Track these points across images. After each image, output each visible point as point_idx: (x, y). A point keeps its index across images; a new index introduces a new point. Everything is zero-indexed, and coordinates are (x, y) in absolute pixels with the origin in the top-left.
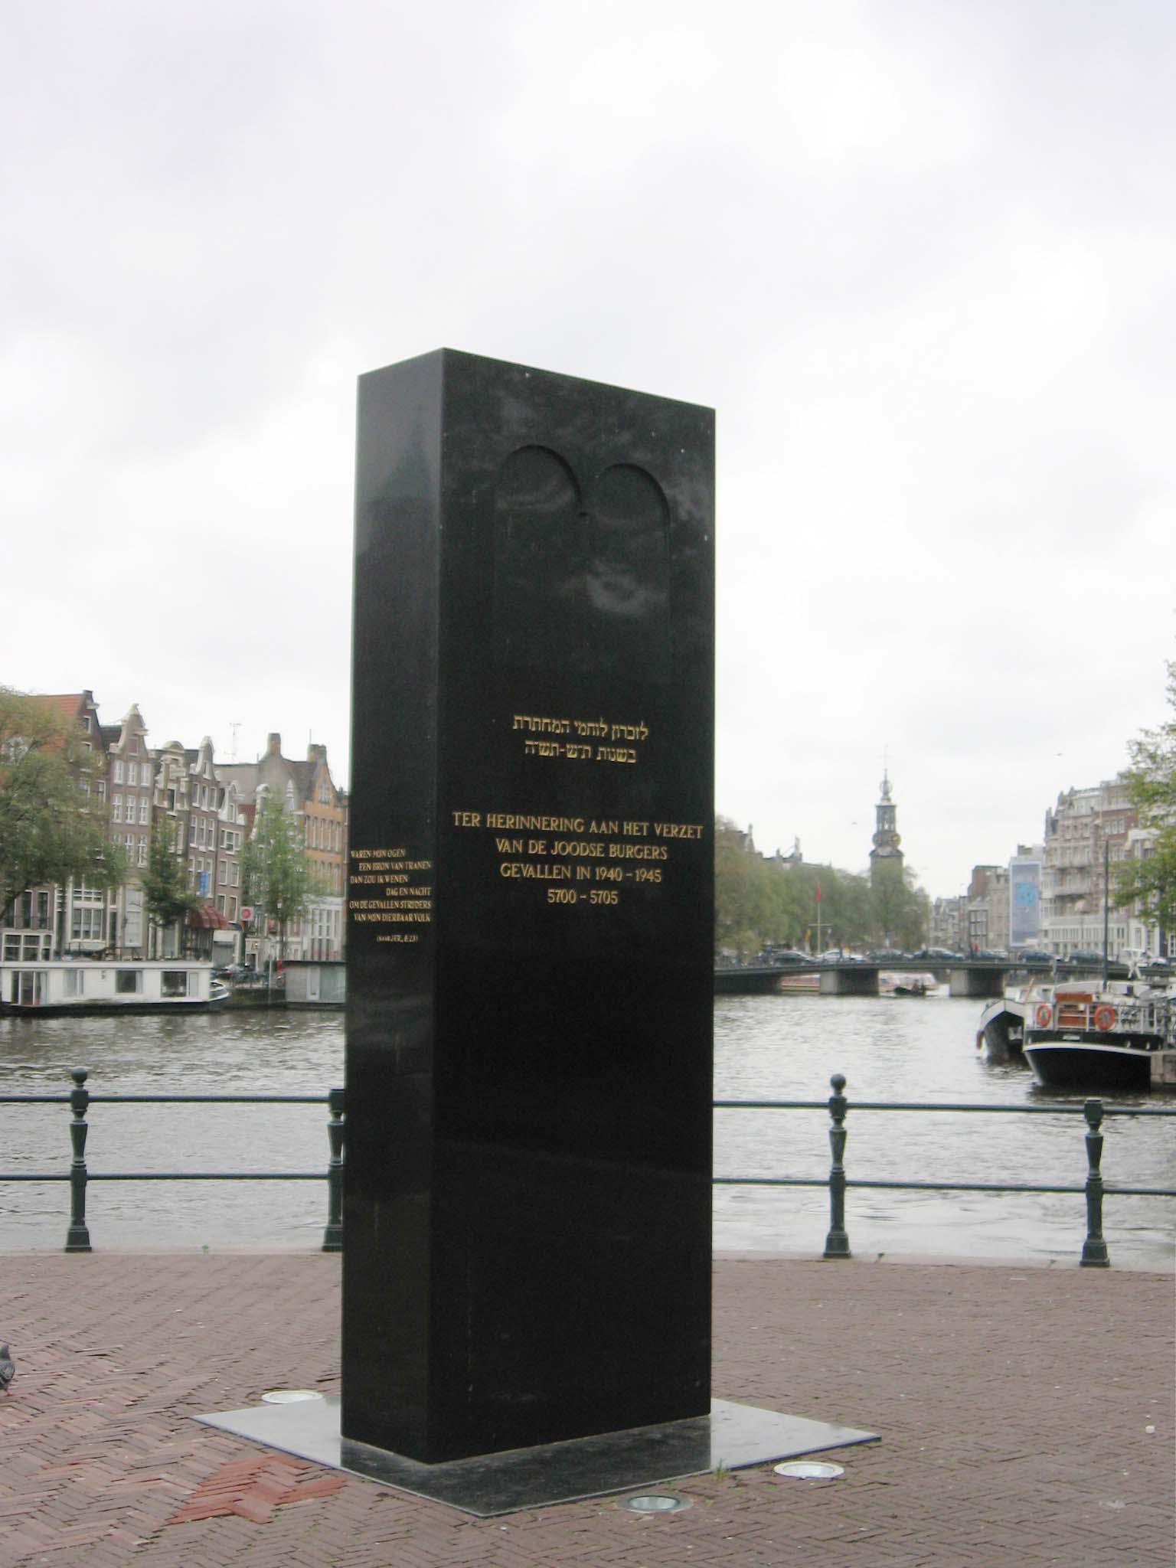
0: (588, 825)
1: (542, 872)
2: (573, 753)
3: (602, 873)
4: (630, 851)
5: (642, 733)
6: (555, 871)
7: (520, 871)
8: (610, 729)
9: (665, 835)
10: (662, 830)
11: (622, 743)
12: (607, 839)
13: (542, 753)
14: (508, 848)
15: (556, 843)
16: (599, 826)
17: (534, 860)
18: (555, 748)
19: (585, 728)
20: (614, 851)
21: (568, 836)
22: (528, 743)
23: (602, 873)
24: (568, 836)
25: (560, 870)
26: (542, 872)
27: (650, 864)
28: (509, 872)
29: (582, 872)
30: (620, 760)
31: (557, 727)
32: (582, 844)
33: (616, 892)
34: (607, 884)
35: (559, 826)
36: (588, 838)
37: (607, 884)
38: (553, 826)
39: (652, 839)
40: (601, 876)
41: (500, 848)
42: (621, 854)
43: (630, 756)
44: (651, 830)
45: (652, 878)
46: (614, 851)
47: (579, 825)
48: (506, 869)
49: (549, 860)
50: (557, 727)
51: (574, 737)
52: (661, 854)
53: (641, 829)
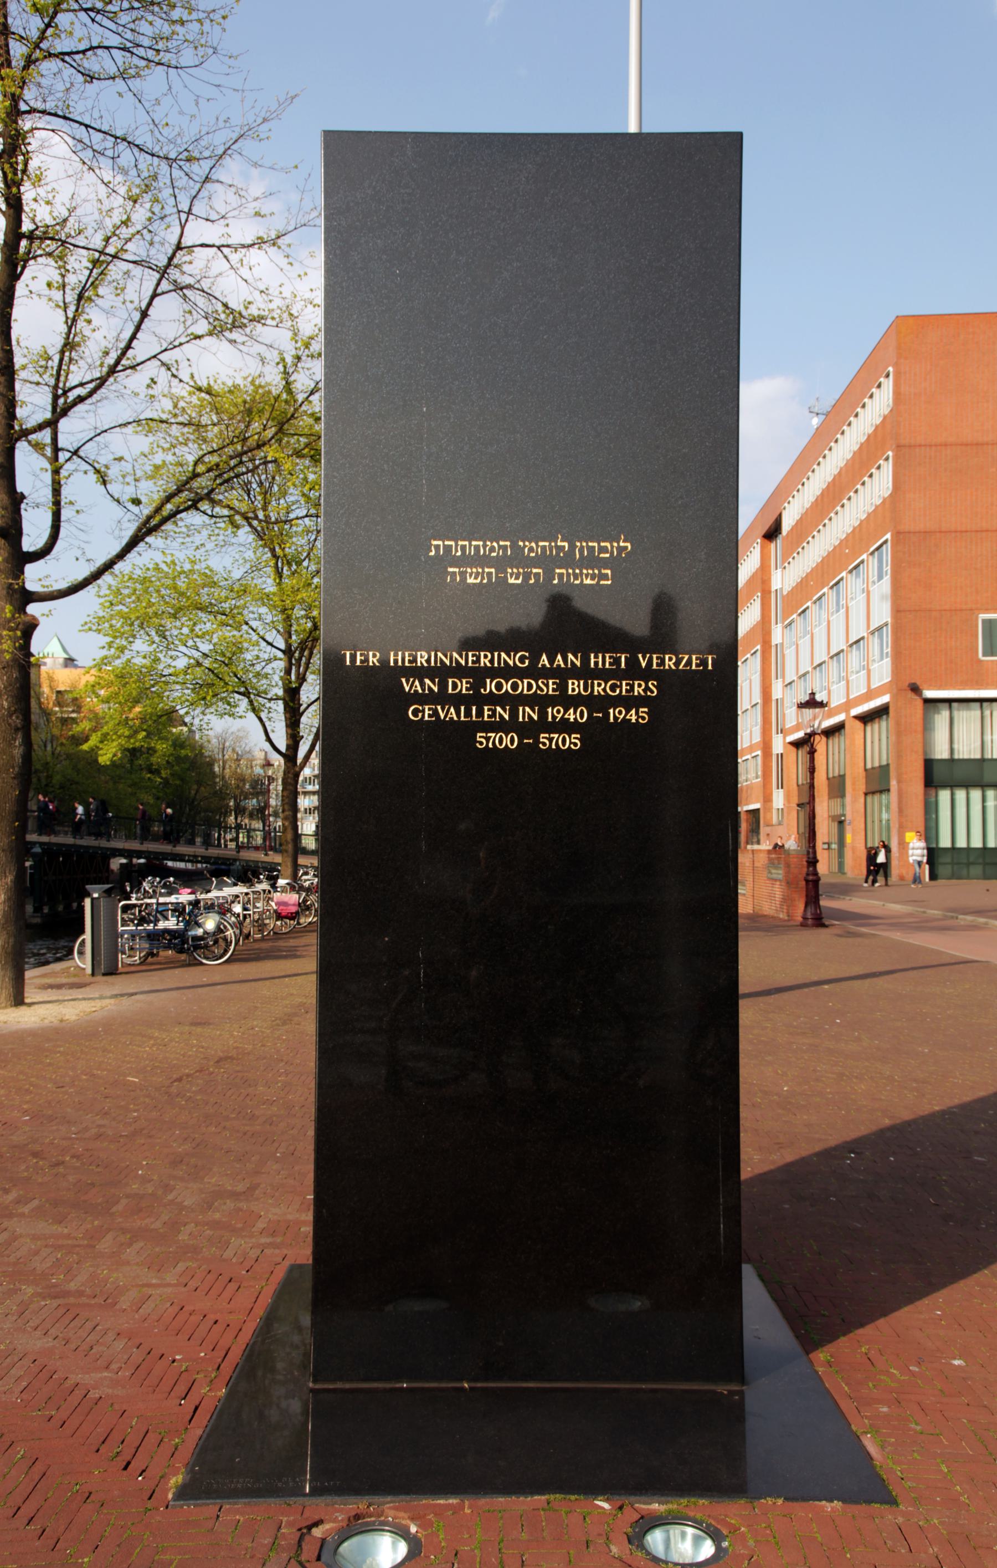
0: (535, 658)
1: (468, 713)
2: (517, 578)
3: (553, 713)
4: (599, 688)
5: (621, 549)
6: (486, 713)
7: (435, 713)
8: (573, 547)
9: (655, 667)
10: (650, 660)
11: (591, 561)
12: (562, 675)
13: (470, 581)
14: (419, 689)
15: (488, 681)
16: (552, 660)
17: (457, 700)
18: (490, 574)
19: (531, 548)
20: (574, 687)
21: (507, 672)
22: (450, 570)
23: (553, 713)
24: (507, 672)
25: (494, 711)
26: (468, 713)
27: (630, 702)
28: (420, 715)
29: (527, 713)
30: (588, 581)
31: (492, 550)
32: (526, 681)
33: (578, 736)
34: (565, 727)
35: (492, 661)
36: (534, 672)
37: (565, 727)
38: (484, 662)
39: (634, 672)
40: (554, 717)
41: (407, 689)
42: (586, 690)
43: (605, 577)
44: (632, 662)
45: (634, 719)
46: (574, 687)
47: (522, 660)
48: (415, 713)
49: (478, 699)
50: (492, 550)
51: (518, 559)
52: (647, 689)
53: (617, 661)
